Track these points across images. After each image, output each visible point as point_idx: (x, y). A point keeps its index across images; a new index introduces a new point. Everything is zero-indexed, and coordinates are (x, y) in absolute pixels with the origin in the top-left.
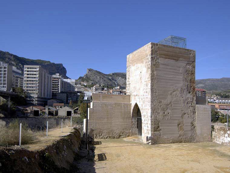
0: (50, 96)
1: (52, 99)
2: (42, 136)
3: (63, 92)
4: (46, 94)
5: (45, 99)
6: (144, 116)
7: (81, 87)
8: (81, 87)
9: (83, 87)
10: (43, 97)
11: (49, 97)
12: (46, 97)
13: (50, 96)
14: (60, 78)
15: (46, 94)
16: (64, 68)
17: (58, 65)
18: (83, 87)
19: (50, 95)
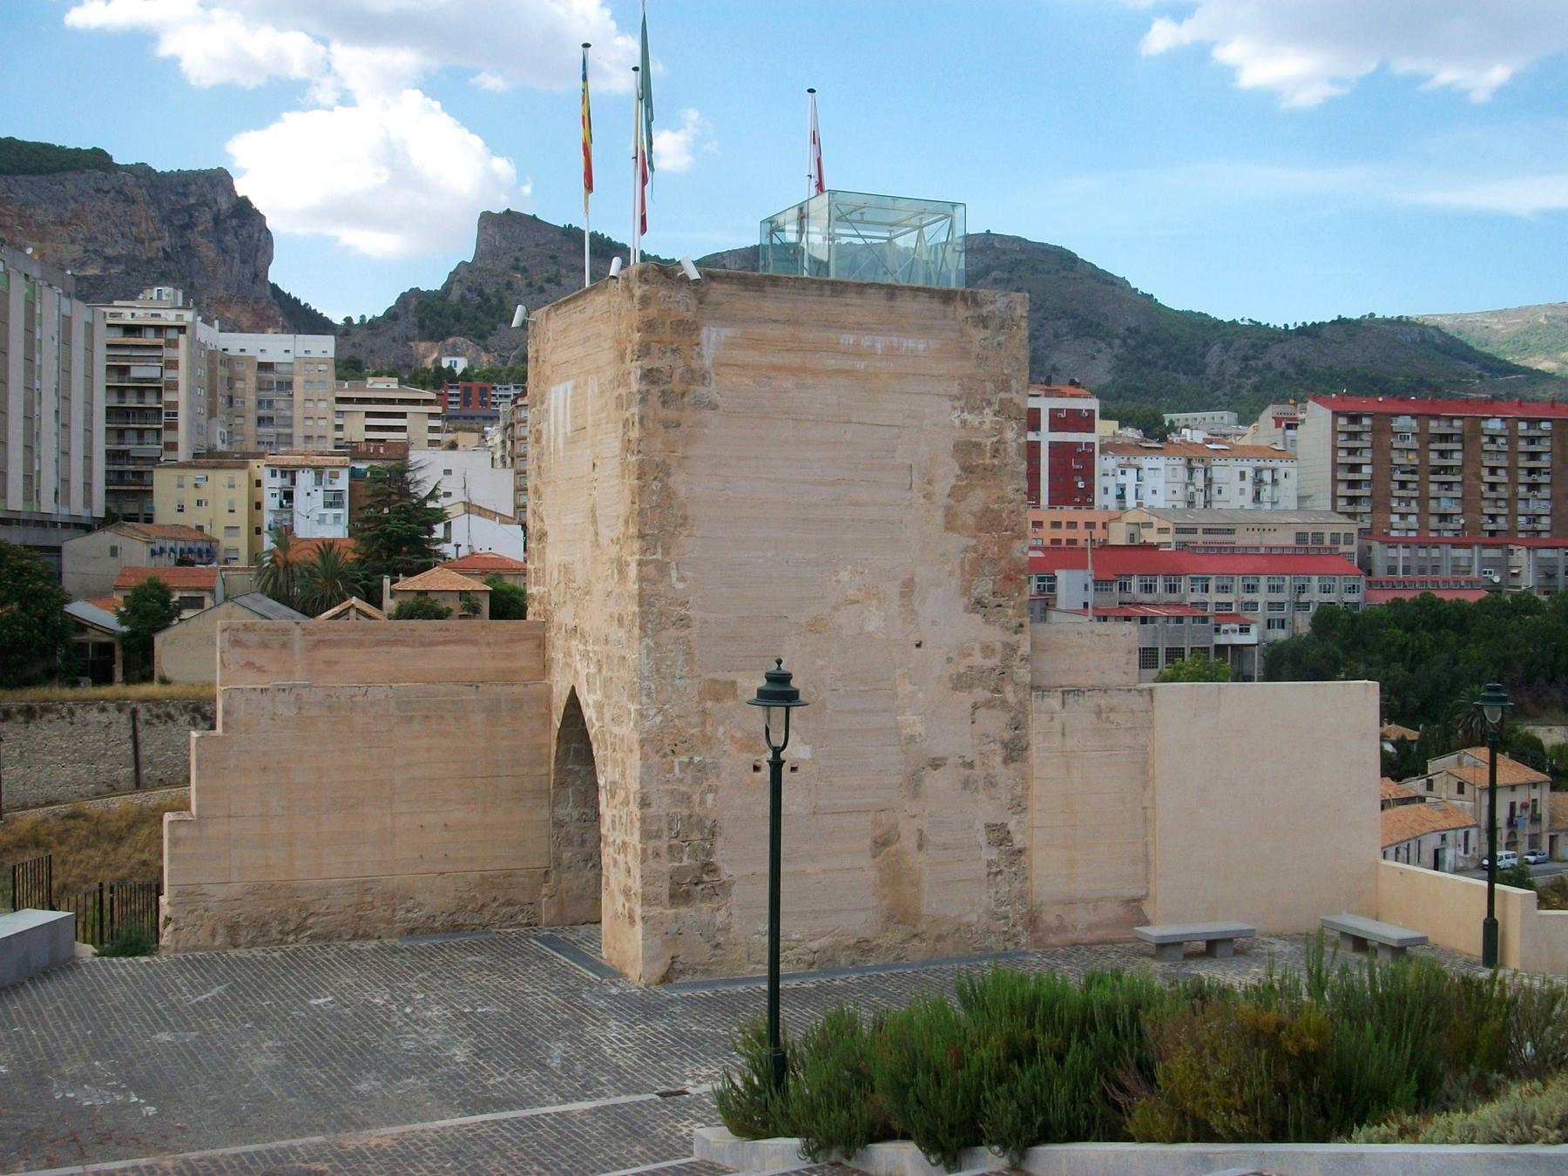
0: (88, 503)
1: (110, 520)
2: (1033, 1076)
3: (211, 453)
4: (48, 483)
5: (44, 523)
6: (1459, 762)
7: (402, 401)
8: (402, 401)
9: (428, 402)
10: (19, 508)
11: (77, 508)
12: (48, 505)
13: (88, 503)
14: (182, 329)
15: (48, 483)
16: (245, 211)
17: (182, 182)
18: (428, 402)
19: (88, 486)
